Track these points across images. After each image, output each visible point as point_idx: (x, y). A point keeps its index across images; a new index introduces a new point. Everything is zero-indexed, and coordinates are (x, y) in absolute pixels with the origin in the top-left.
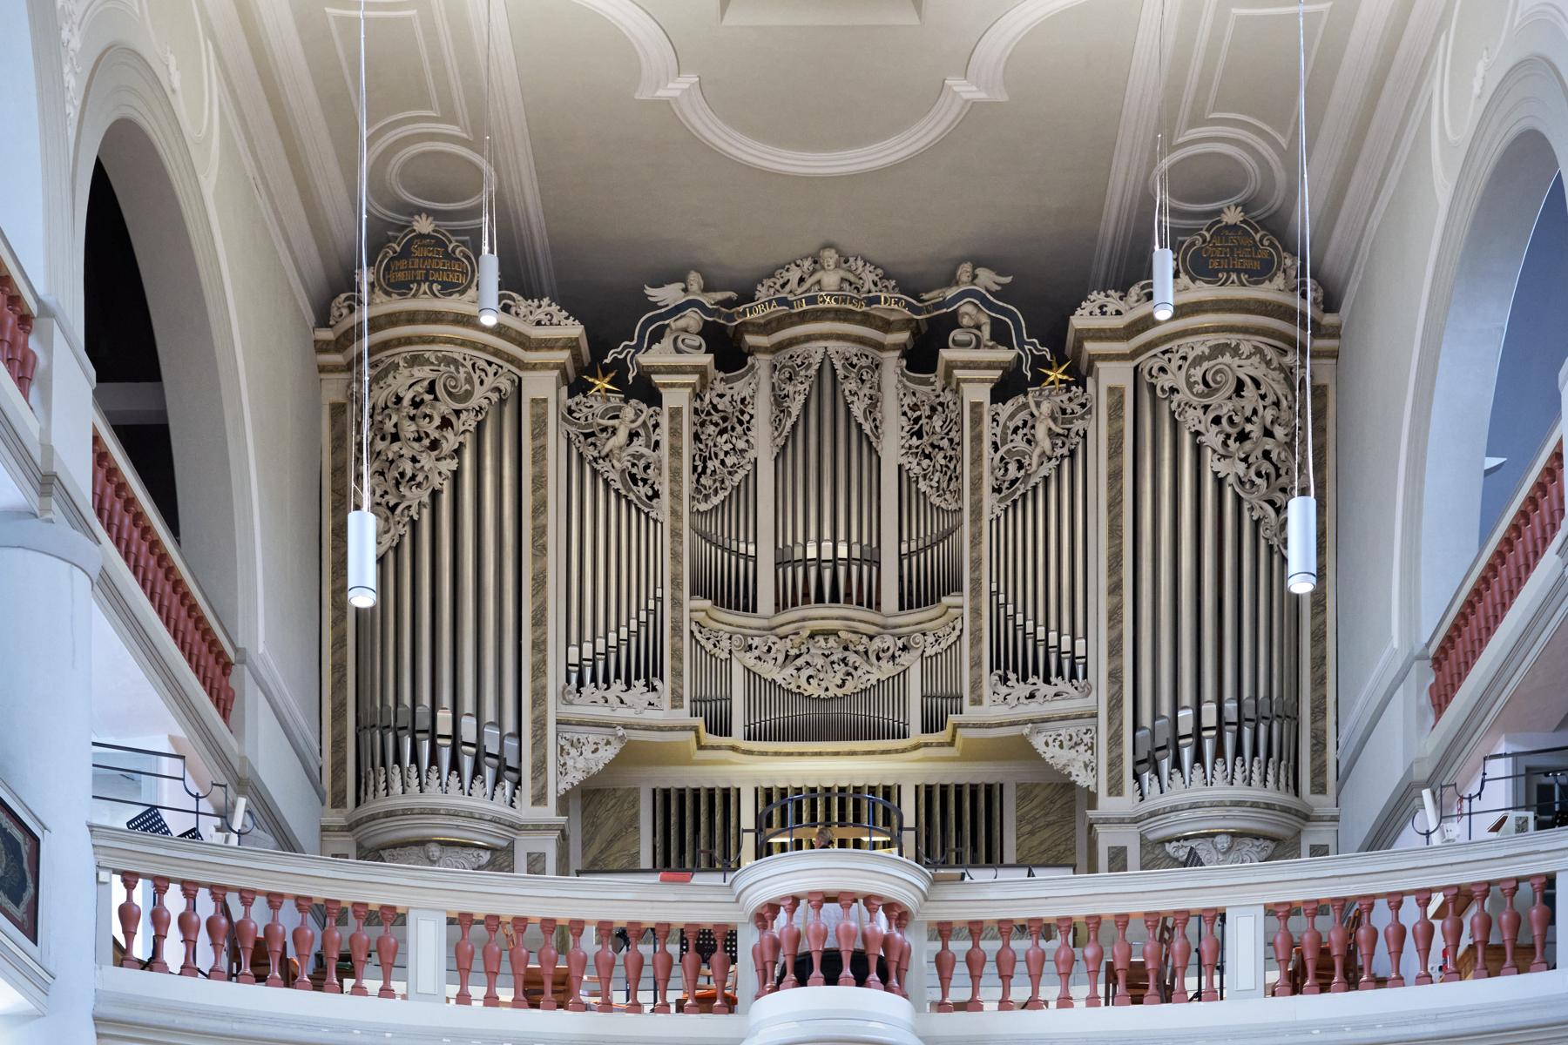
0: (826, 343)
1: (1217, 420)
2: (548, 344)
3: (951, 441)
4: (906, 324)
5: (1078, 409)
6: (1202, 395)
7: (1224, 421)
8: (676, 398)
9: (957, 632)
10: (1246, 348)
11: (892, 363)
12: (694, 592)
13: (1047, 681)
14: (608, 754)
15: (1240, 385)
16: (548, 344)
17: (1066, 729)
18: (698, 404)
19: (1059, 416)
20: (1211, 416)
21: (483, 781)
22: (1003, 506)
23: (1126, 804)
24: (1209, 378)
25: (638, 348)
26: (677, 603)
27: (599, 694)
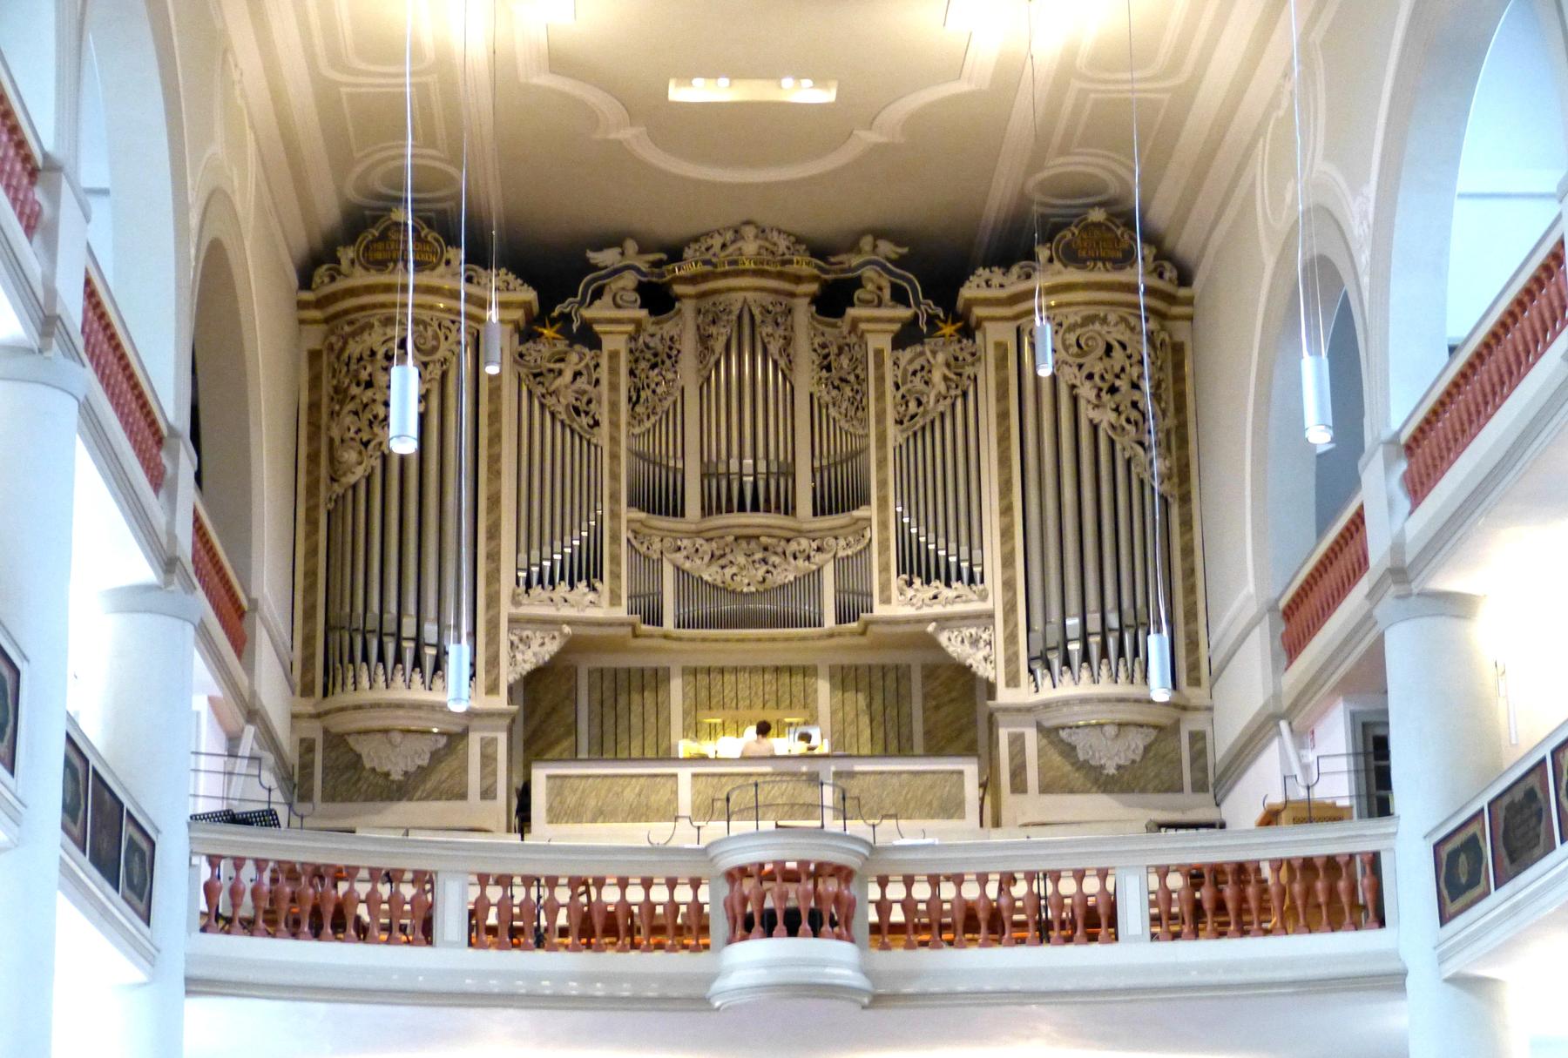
0: (744, 292)
3: (857, 377)
4: (814, 279)
5: (969, 359)
8: (615, 341)
11: (803, 312)
13: (948, 584)
14: (552, 647)
18: (633, 345)
19: (952, 361)
23: (1023, 695)
25: (581, 303)
26: (615, 515)
27: (546, 594)
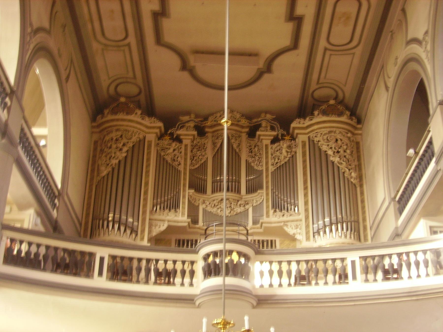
1: (331, 148)
2: (154, 128)
3: (260, 154)
5: (294, 146)
6: (326, 142)
7: (333, 148)
8: (187, 141)
9: (262, 200)
10: (338, 132)
12: (190, 187)
15: (337, 140)
16: (154, 128)
17: (293, 224)
20: (330, 147)
21: (127, 234)
22: (274, 168)
24: (329, 138)
25: (177, 130)
